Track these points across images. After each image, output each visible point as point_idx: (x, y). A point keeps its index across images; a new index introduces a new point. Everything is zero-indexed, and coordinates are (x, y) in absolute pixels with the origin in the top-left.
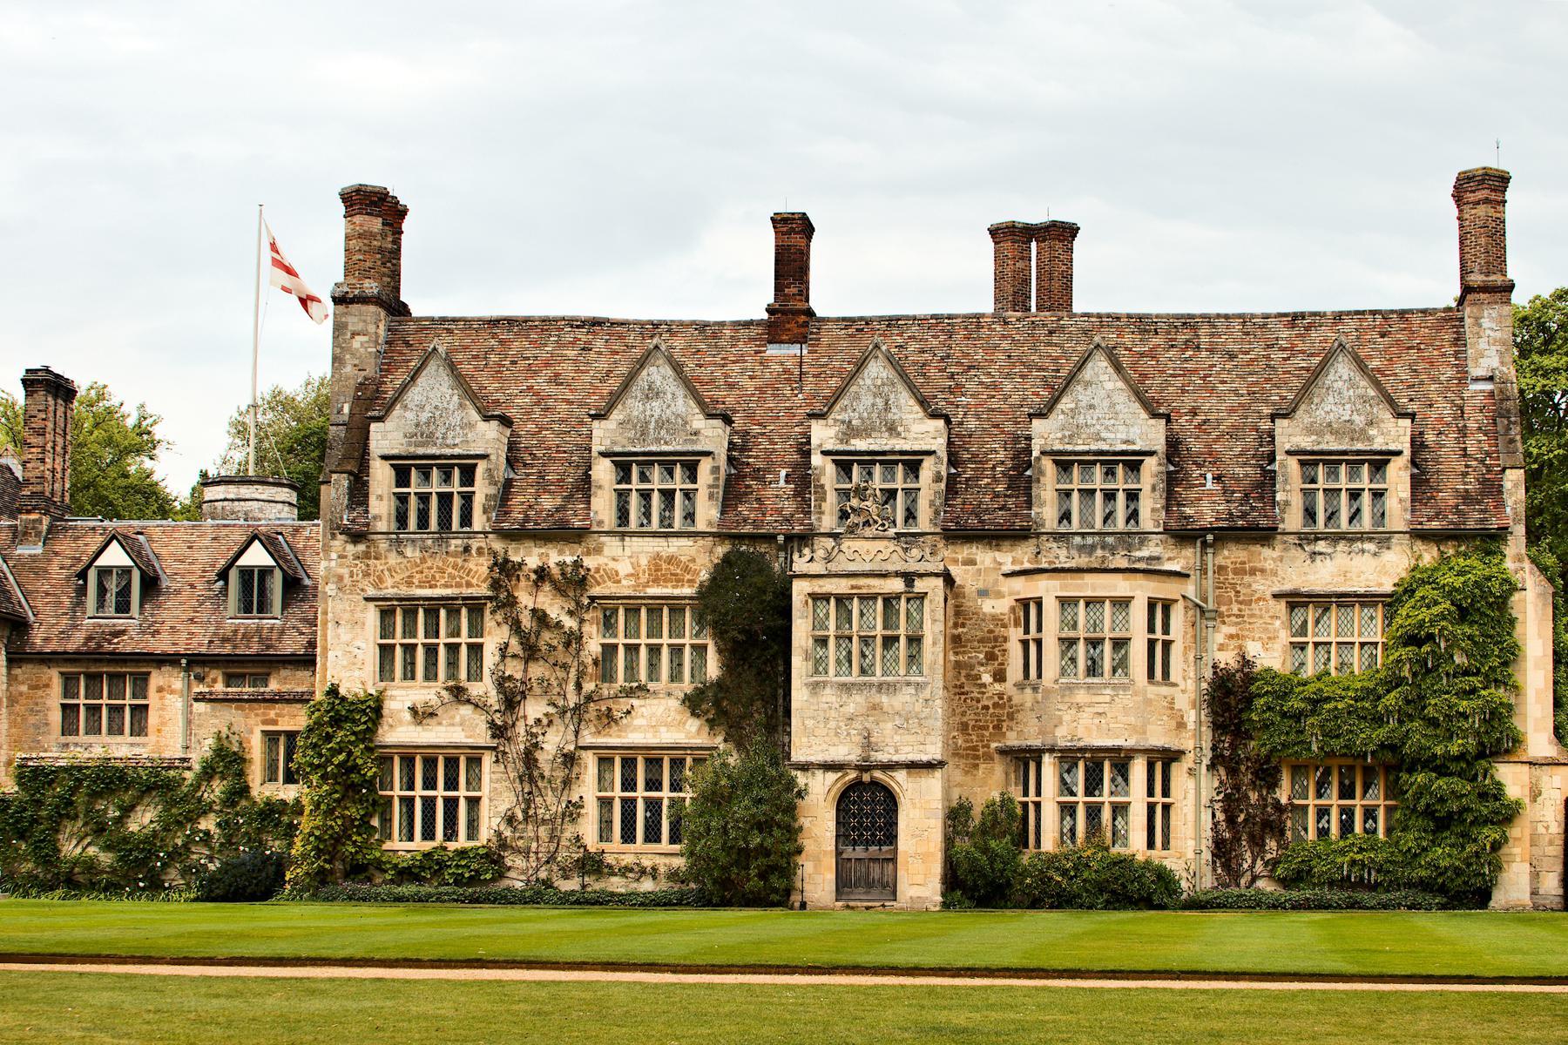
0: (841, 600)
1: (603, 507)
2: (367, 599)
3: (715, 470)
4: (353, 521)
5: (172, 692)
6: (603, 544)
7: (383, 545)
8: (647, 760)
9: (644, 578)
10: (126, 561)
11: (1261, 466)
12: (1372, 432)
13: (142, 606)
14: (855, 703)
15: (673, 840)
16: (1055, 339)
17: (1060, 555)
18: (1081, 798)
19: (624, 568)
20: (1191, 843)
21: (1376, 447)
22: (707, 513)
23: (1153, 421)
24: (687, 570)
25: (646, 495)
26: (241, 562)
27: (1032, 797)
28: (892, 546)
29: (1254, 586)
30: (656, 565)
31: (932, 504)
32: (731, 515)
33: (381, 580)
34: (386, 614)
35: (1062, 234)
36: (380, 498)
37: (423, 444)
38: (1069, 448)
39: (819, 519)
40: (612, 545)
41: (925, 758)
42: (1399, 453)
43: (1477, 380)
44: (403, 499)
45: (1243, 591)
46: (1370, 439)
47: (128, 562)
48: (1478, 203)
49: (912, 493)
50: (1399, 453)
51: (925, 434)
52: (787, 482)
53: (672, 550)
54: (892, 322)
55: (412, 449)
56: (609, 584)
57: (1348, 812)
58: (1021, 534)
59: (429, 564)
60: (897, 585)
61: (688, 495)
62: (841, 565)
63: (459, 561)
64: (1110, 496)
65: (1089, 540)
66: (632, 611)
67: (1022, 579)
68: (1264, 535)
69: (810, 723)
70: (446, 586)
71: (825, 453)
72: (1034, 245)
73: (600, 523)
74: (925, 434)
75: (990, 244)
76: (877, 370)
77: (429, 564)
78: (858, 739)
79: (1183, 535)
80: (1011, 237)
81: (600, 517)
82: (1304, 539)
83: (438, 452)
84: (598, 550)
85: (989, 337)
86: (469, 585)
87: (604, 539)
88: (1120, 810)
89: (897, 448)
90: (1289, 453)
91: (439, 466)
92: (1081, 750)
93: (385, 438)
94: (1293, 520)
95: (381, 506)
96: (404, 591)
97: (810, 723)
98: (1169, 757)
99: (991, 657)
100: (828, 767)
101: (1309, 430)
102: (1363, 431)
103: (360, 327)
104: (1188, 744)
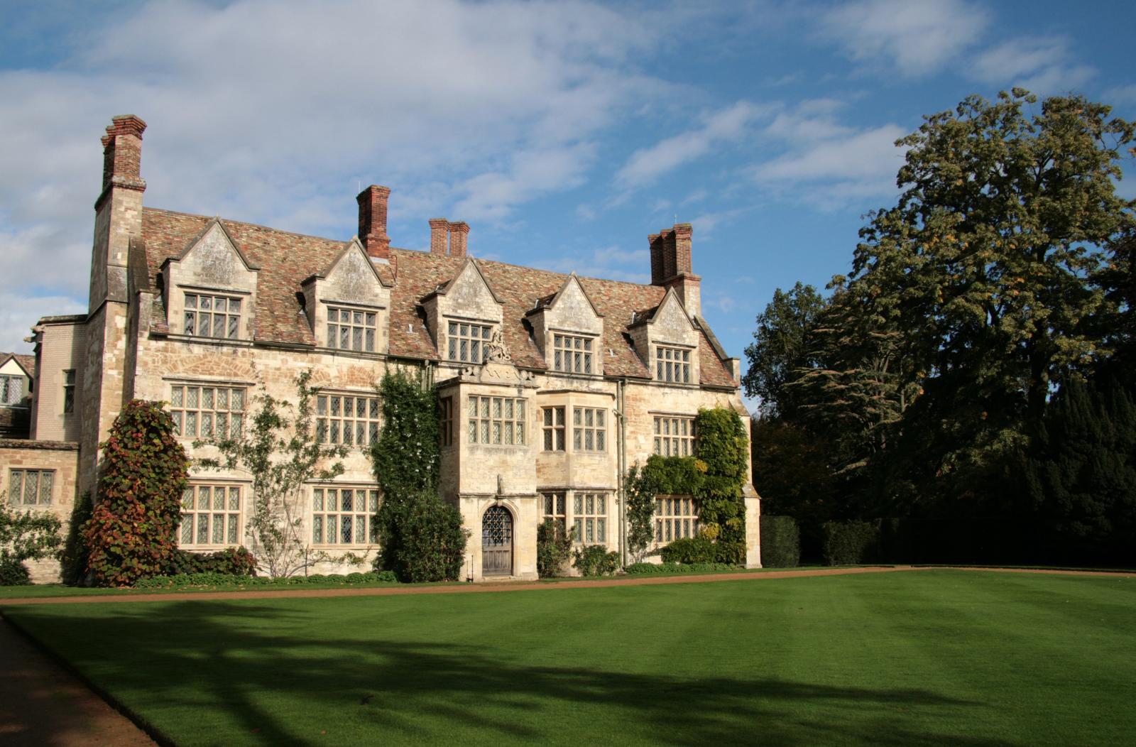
2: (164, 379)
4: (156, 326)
8: (342, 491)
9: (345, 379)
12: (685, 336)
14: (493, 459)
15: (358, 541)
17: (558, 384)
19: (333, 373)
21: (686, 343)
22: (381, 344)
23: (598, 319)
25: (344, 330)
27: (555, 515)
28: (513, 371)
29: (641, 408)
30: (352, 372)
33: (175, 367)
34: (175, 388)
36: (176, 312)
37: (206, 281)
38: (561, 328)
39: (442, 353)
40: (327, 359)
41: (529, 492)
44: (190, 316)
46: (684, 339)
51: (493, 312)
55: (200, 284)
57: (677, 522)
58: (541, 372)
60: (513, 392)
61: (370, 333)
62: (486, 377)
63: (230, 359)
64: (577, 355)
67: (547, 396)
68: (644, 380)
69: (469, 470)
70: (220, 375)
71: (444, 316)
73: (321, 343)
74: (493, 312)
76: (469, 273)
77: (209, 359)
81: (320, 339)
83: (217, 287)
84: (319, 361)
86: (236, 375)
89: (482, 317)
90: (653, 342)
91: (218, 297)
92: (587, 489)
93: (181, 274)
94: (655, 378)
96: (191, 376)
97: (469, 470)
102: (681, 336)
103: (132, 205)
104: (616, 487)
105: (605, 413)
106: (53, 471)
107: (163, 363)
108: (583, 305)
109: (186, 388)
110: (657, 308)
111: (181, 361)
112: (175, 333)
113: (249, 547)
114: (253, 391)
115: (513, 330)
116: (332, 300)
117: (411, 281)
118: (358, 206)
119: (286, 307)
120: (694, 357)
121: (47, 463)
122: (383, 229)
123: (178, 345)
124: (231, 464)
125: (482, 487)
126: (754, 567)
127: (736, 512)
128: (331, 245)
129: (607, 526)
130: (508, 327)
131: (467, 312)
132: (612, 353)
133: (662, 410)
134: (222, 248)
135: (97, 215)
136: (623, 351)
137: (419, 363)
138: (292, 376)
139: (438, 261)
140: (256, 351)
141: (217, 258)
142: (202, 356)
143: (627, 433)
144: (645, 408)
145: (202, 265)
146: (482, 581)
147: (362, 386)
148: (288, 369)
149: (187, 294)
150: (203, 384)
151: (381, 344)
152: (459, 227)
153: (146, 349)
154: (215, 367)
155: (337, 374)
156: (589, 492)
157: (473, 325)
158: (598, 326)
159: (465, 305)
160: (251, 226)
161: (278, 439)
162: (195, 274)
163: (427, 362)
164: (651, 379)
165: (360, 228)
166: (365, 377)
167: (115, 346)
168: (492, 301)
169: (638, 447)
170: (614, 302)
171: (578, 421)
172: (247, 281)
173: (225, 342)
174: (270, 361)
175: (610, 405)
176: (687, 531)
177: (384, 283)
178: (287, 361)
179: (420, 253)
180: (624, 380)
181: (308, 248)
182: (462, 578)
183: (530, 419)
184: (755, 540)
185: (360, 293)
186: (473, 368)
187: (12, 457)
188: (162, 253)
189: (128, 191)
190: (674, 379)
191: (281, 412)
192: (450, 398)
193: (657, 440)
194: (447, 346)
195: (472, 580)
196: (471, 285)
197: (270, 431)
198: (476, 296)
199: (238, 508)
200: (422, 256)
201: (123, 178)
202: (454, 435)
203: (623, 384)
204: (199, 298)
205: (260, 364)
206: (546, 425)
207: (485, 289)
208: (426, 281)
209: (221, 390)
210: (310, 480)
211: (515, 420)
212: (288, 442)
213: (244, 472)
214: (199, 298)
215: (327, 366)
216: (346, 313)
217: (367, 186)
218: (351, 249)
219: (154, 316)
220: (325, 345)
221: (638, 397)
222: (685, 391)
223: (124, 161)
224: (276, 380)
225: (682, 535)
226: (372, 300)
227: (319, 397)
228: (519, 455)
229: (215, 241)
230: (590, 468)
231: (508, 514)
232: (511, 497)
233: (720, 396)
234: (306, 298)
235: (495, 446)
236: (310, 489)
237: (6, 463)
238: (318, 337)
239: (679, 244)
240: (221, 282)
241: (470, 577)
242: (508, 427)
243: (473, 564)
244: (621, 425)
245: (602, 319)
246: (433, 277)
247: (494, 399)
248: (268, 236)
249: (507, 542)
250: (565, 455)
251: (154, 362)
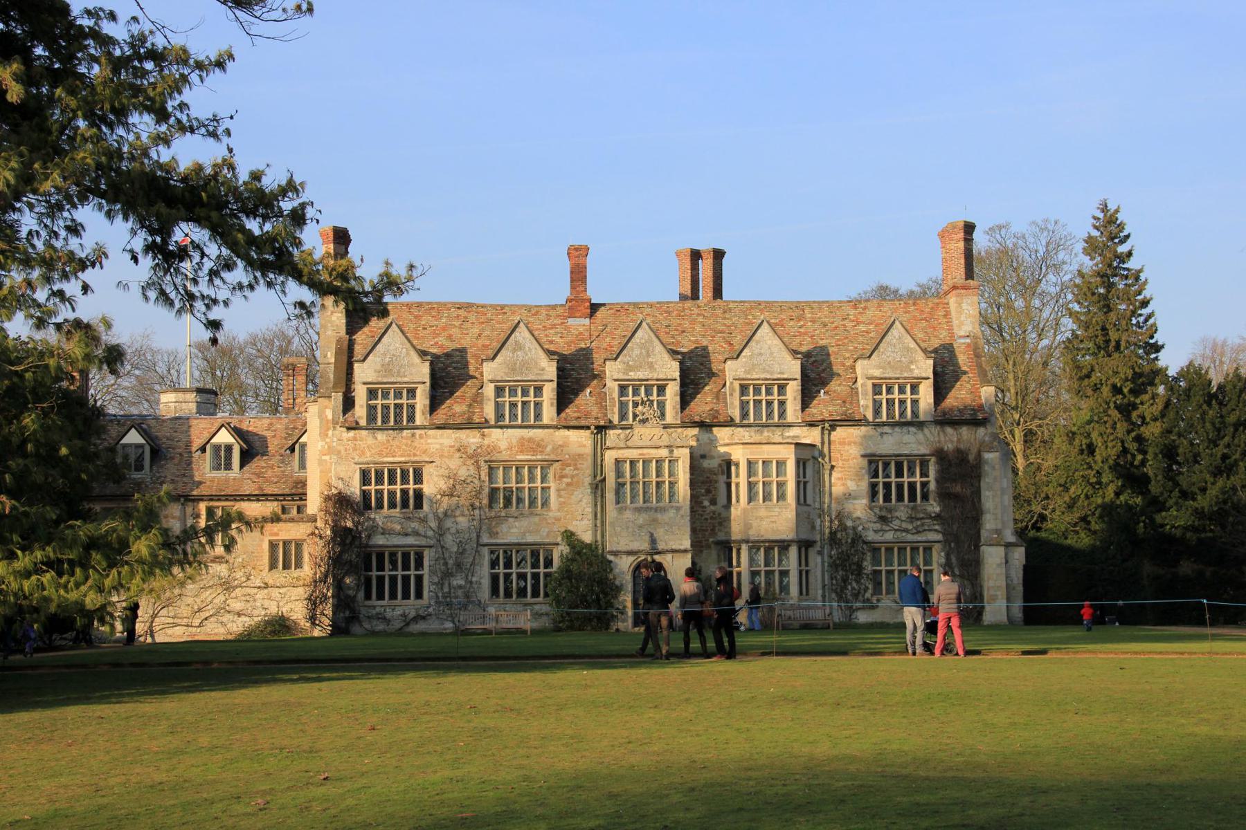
1: (489, 411)
5: (174, 518)
10: (141, 440)
13: (151, 466)
16: (727, 316)
18: (762, 568)
19: (503, 445)
20: (820, 592)
22: (549, 413)
24: (539, 445)
26: (214, 440)
31: (674, 408)
32: (563, 415)
33: (363, 453)
36: (362, 406)
40: (496, 432)
41: (682, 548)
46: (911, 370)
47: (141, 440)
49: (661, 405)
54: (636, 305)
55: (380, 380)
60: (664, 453)
61: (538, 405)
64: (769, 403)
69: (618, 529)
78: (647, 538)
79: (812, 424)
86: (415, 455)
88: (784, 573)
93: (364, 373)
95: (360, 411)
96: (378, 459)
99: (708, 491)
100: (630, 553)
101: (879, 367)
108: (775, 350)
123: (364, 433)
133: (879, 452)
136: (839, 389)
139: (648, 311)
170: (862, 327)
174: (447, 438)
179: (629, 304)
194: (616, 410)
196: (642, 346)
198: (648, 356)
200: (631, 308)
216: (513, 392)
222: (912, 429)
228: (672, 513)
233: (964, 431)
240: (399, 375)
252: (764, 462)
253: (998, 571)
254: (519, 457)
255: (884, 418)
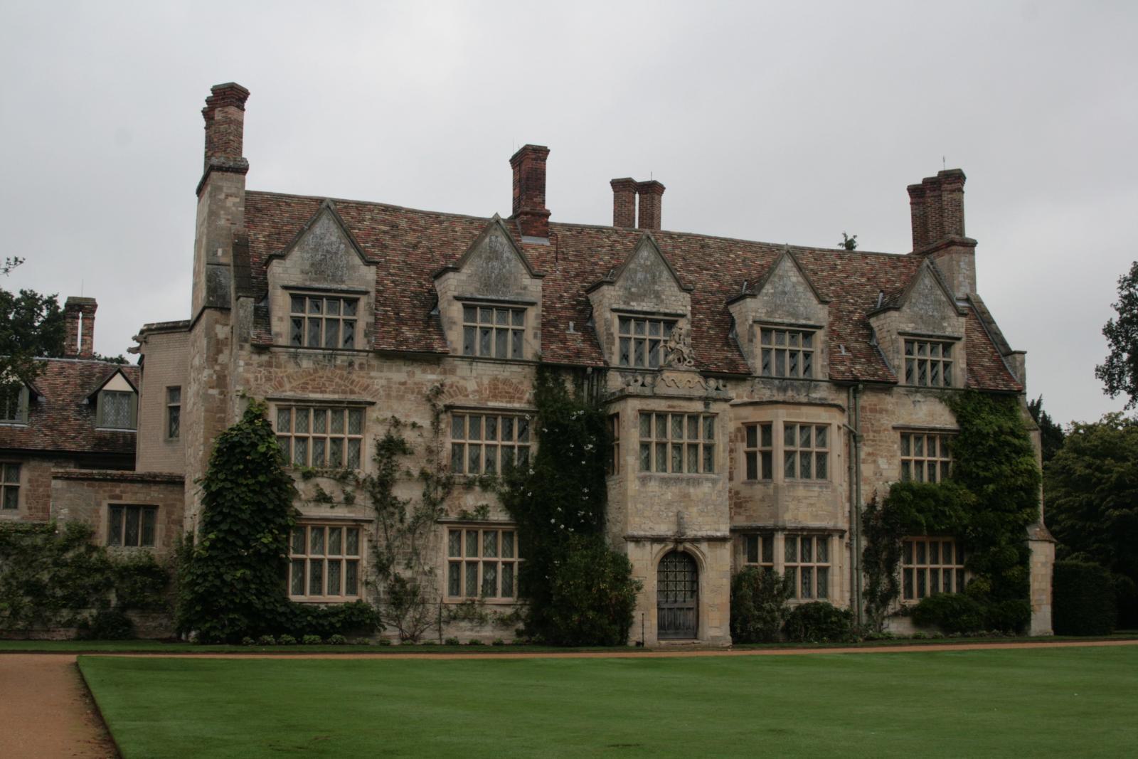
0: (662, 416)
3: (537, 316)
4: (259, 337)
6: (456, 366)
7: (283, 357)
11: (866, 342)
12: (945, 324)
14: (670, 493)
15: (505, 594)
19: (471, 386)
21: (947, 334)
23: (820, 306)
24: (516, 389)
27: (761, 562)
28: (697, 378)
29: (882, 421)
30: (495, 385)
33: (281, 385)
35: (652, 190)
36: (281, 319)
37: (316, 280)
38: (771, 320)
40: (463, 368)
41: (719, 534)
42: (959, 339)
43: (959, 300)
44: (297, 322)
45: (876, 424)
46: (944, 328)
48: (954, 191)
50: (959, 339)
51: (679, 302)
52: (575, 329)
53: (507, 374)
55: (308, 284)
56: (460, 397)
59: (320, 374)
60: (698, 407)
62: (661, 389)
63: (345, 373)
64: (793, 354)
65: (784, 383)
66: (475, 418)
68: (886, 386)
69: (640, 506)
70: (334, 392)
72: (637, 196)
73: (455, 350)
74: (679, 302)
75: (610, 193)
76: (646, 254)
77: (320, 374)
78: (674, 519)
79: (839, 385)
80: (623, 187)
82: (912, 390)
83: (329, 287)
84: (453, 371)
85: (665, 245)
86: (352, 392)
87: (458, 362)
90: (900, 334)
91: (329, 298)
92: (803, 529)
93: (285, 273)
94: (902, 380)
96: (300, 394)
97: (640, 506)
98: (841, 533)
103: (233, 190)
104: (846, 527)
105: (828, 431)
106: (157, 507)
107: (266, 380)
109: (294, 410)
110: (901, 291)
111: (288, 377)
112: (279, 344)
113: (370, 600)
114: (373, 411)
115: (708, 323)
116: (468, 295)
117: (576, 265)
118: (512, 171)
119: (414, 306)
120: (959, 355)
121: (148, 498)
122: (540, 200)
124: (349, 501)
125: (657, 527)
126: (1040, 634)
127: (1016, 558)
128: (476, 224)
129: (830, 577)
130: (701, 320)
131: (644, 304)
132: (844, 353)
133: (913, 424)
134: (334, 239)
135: (199, 201)
136: (857, 345)
137: (579, 373)
138: (419, 393)
139: (615, 237)
140: (375, 362)
141: (328, 251)
142: (312, 371)
143: (862, 455)
144: (888, 421)
145: (310, 261)
146: (657, 645)
147: (507, 402)
148: (415, 383)
149: (293, 297)
150: (314, 404)
151: (532, 347)
152: (652, 190)
153: (247, 364)
154: (327, 384)
155: (476, 387)
156: (805, 533)
157: (651, 320)
158: (820, 316)
159: (640, 296)
160: (376, 205)
161: (404, 469)
162: (302, 272)
163: (590, 370)
164: (895, 384)
165: (514, 199)
166: (511, 390)
167: (216, 360)
168: (676, 289)
169: (878, 473)
170: (853, 279)
171: (789, 440)
172: (366, 276)
173: (339, 352)
175: (836, 420)
176: (947, 585)
177: (533, 272)
178: (414, 373)
179: (591, 227)
180: (857, 386)
181: (446, 228)
182: (631, 643)
183: (721, 441)
184: (1044, 597)
185: (504, 285)
186: (644, 378)
187: (111, 491)
188: (269, 247)
189: (229, 174)
190: (929, 384)
191: (409, 436)
192: (617, 415)
193: (905, 464)
194: (616, 347)
195: (643, 644)
196: (646, 269)
197: (395, 458)
198: (654, 283)
199: (357, 554)
201: (222, 160)
202: (621, 462)
203: (856, 391)
204: (307, 300)
205: (381, 378)
206: (748, 447)
207: (666, 274)
208: (596, 264)
209: (335, 411)
210: (444, 519)
211: (701, 440)
212: (416, 473)
213: (363, 508)
214: (307, 300)
215: (464, 378)
217: (522, 146)
218: (492, 231)
219: (256, 324)
220: (460, 352)
221: (878, 407)
223: (225, 138)
224: (401, 398)
225: (941, 589)
226: (518, 294)
227: (454, 416)
228: (706, 488)
229: (326, 231)
230: (808, 501)
231: (692, 564)
232: (695, 540)
234: (439, 294)
235: (675, 475)
236: (444, 531)
237: (105, 499)
238: (451, 342)
239: (946, 197)
240: (334, 280)
241: (641, 641)
242: (692, 451)
243: (645, 623)
244: (853, 444)
245: (827, 307)
246: (607, 258)
247: (689, 417)
248: (397, 217)
249: (692, 597)
250: (772, 486)
251: (256, 380)
252: (802, 428)
253: (1043, 572)
254: (491, 404)
255: (916, 382)
